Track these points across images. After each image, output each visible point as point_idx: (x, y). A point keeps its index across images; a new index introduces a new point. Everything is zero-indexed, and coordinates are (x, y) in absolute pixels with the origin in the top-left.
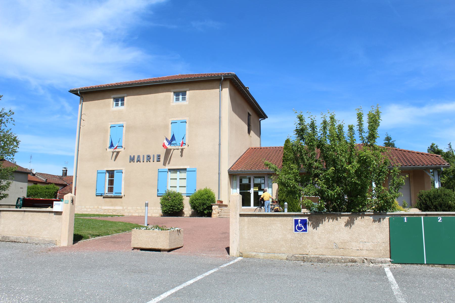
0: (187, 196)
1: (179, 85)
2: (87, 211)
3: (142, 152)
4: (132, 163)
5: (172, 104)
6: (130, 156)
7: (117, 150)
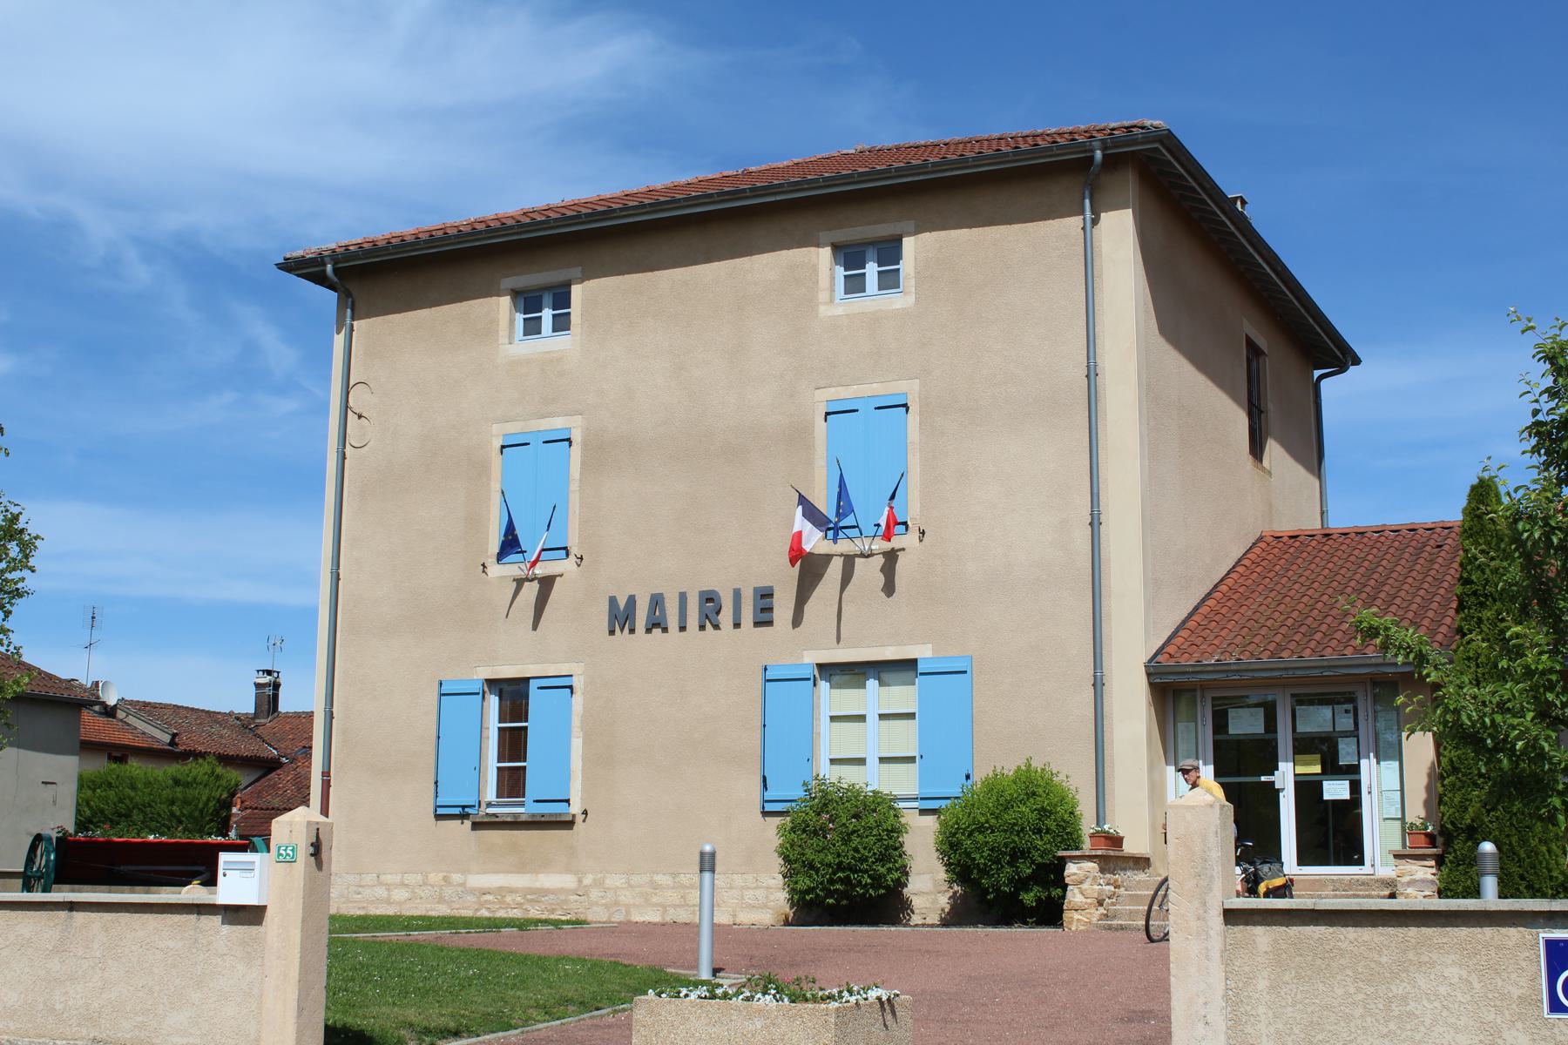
0: (923, 812)
1: (860, 206)
2: (388, 901)
3: (673, 573)
4: (622, 637)
5: (825, 311)
6: (613, 601)
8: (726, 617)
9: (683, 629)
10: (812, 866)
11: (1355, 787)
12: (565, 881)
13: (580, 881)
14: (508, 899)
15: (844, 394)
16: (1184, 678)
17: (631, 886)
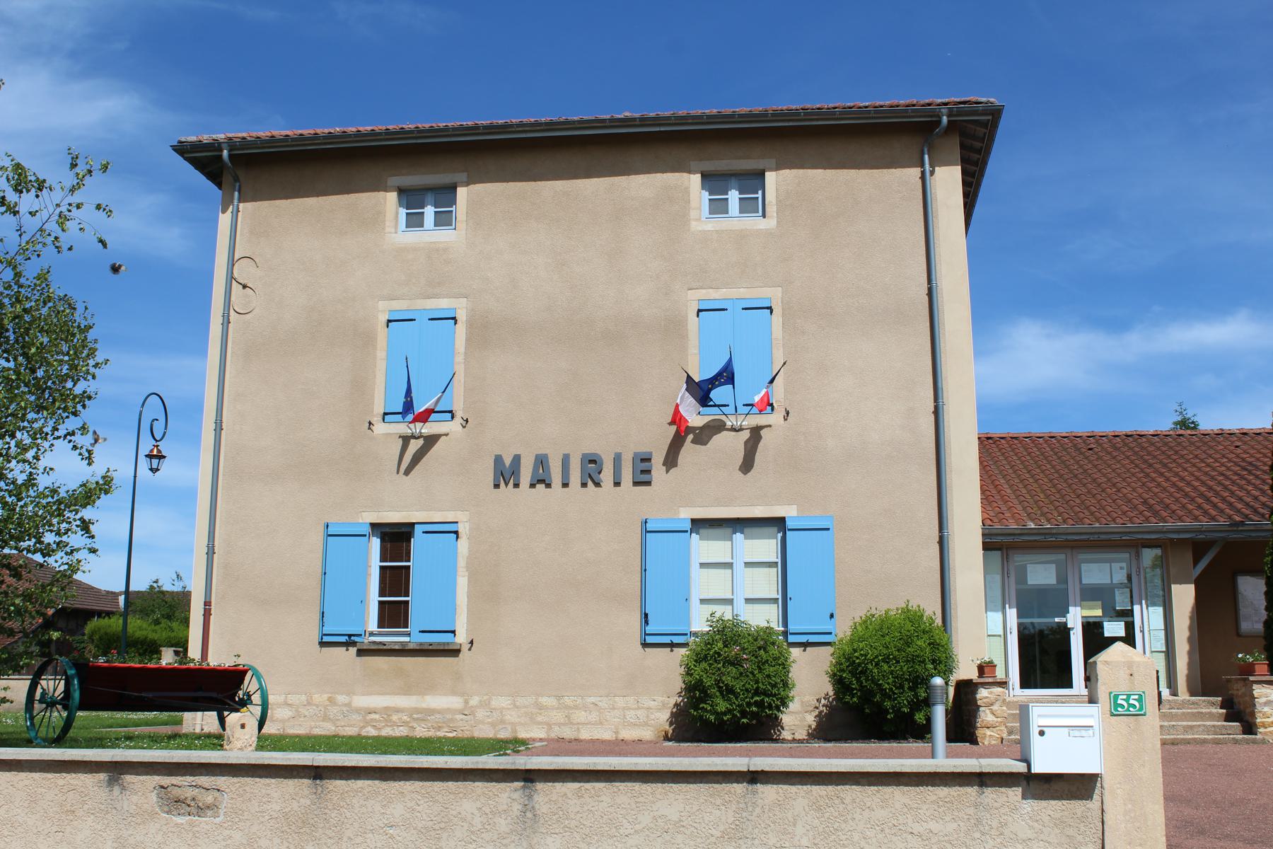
3: (558, 437)
4: (507, 491)
5: (695, 226)
6: (498, 460)
7: (427, 429)
8: (607, 476)
9: (565, 485)
10: (730, 690)
11: (1130, 627)
12: (454, 702)
13: (466, 702)
14: (395, 718)
16: (1010, 539)
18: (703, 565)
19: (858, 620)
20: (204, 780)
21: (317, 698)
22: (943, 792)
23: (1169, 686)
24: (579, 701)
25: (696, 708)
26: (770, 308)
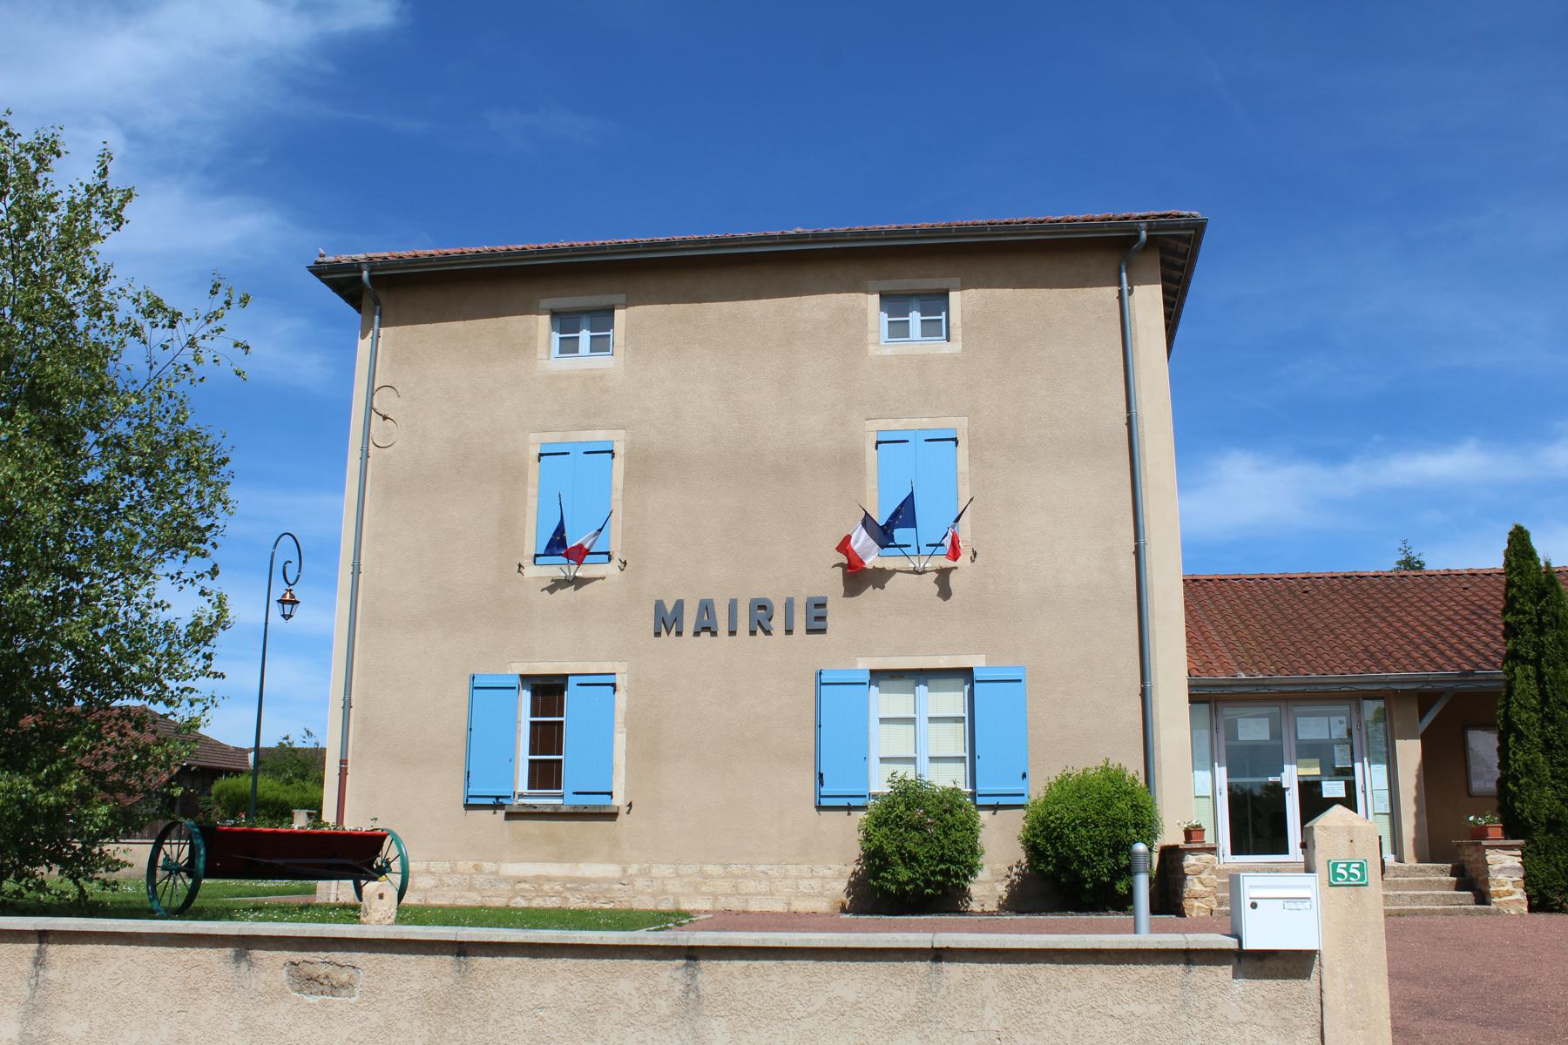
4: (669, 639)
6: (659, 605)
8: (778, 624)
9: (732, 633)
10: (913, 858)
11: (1350, 787)
12: (612, 870)
13: (625, 871)
14: (546, 887)
15: (896, 426)
17: (679, 875)
18: (883, 720)
19: (1053, 780)
20: (339, 956)
21: (462, 866)
22: (1145, 970)
23: (1394, 852)
24: (748, 869)
25: (876, 878)
26: (955, 440)
